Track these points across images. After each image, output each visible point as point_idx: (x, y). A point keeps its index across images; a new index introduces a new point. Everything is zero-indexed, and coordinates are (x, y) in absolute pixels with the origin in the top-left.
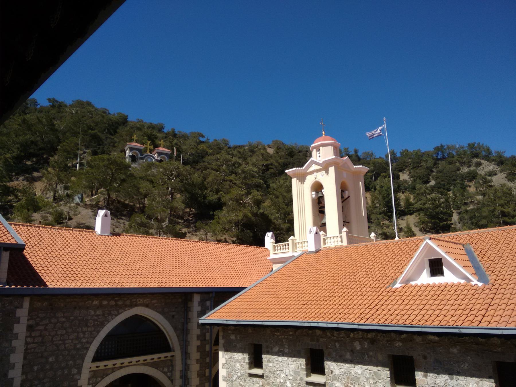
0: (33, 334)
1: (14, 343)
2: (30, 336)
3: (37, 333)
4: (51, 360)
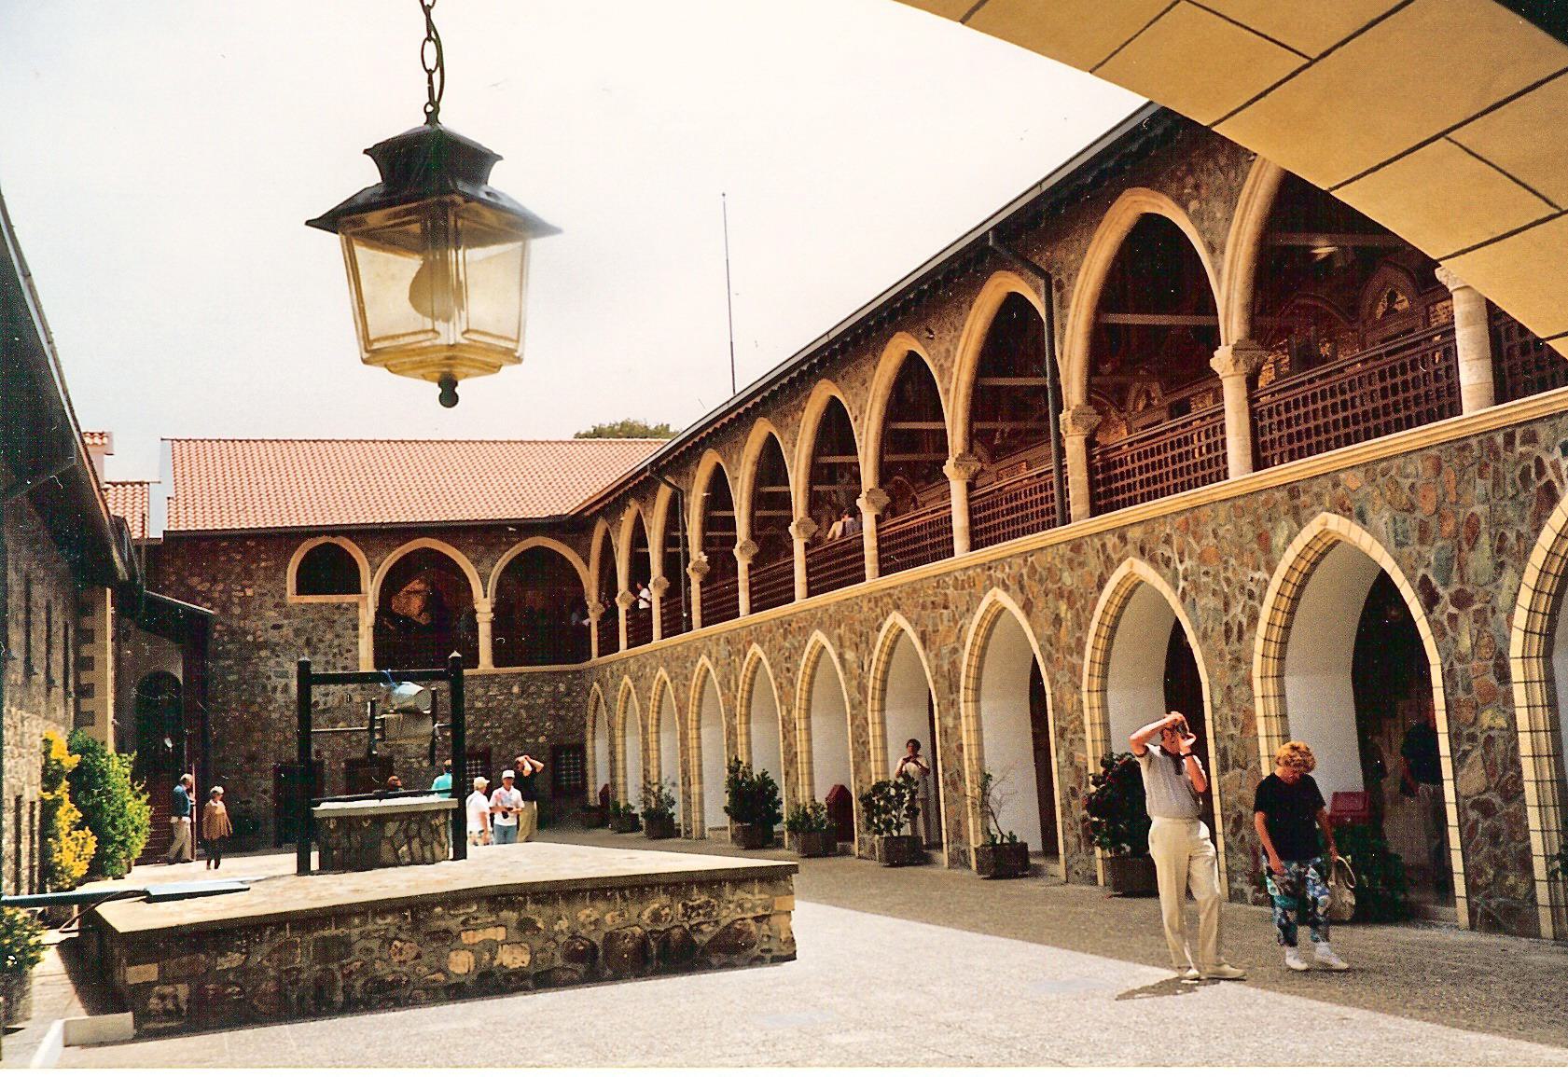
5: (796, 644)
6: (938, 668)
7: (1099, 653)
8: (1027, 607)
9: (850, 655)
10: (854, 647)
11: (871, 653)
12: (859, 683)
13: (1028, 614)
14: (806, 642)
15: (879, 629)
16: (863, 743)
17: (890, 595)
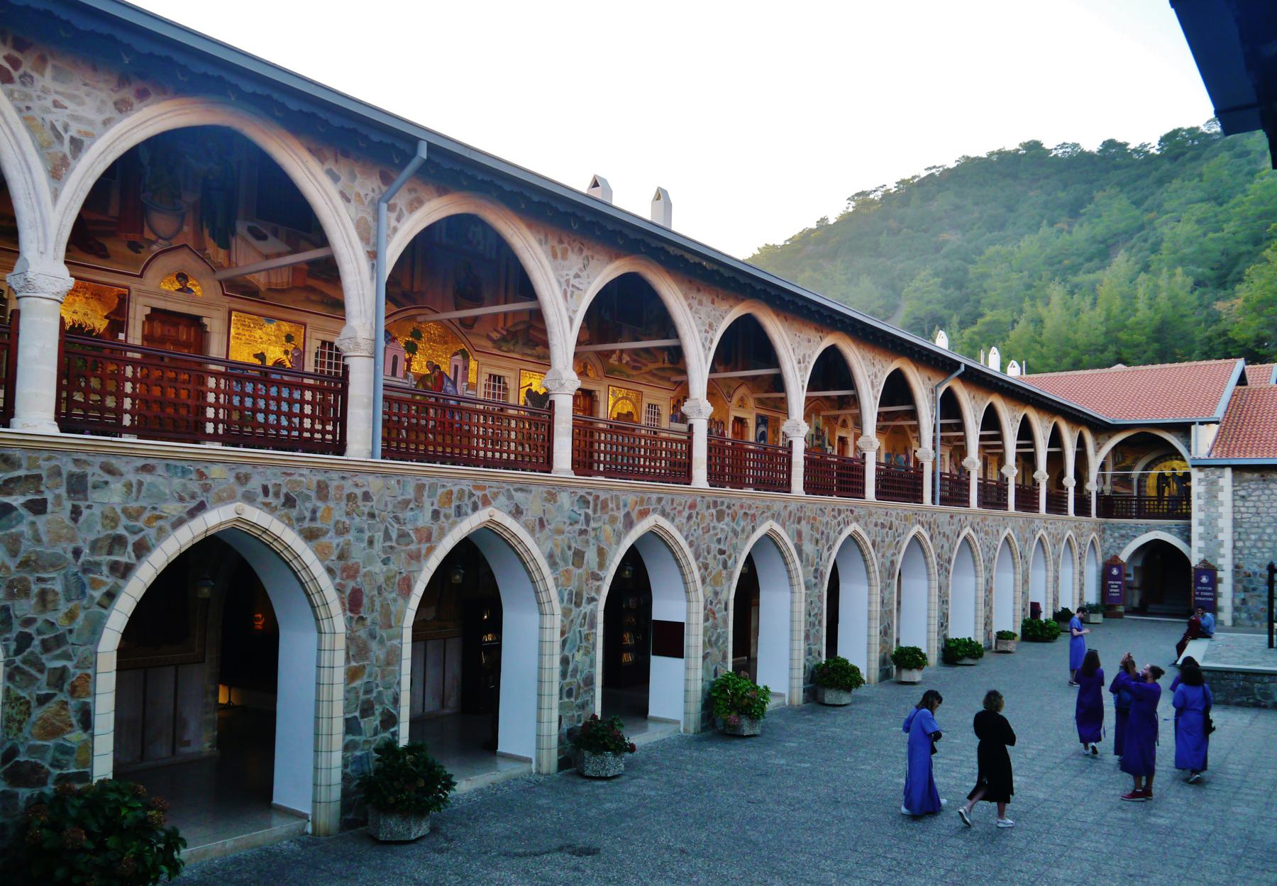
0: (1247, 504)
1: (1221, 509)
2: (1244, 506)
3: (1251, 504)
4: (1269, 531)
5: (739, 529)
8: (931, 538)
9: (808, 548)
10: (814, 542)
11: (830, 548)
12: (816, 570)
13: (931, 540)
14: (754, 529)
15: (840, 532)
16: (816, 615)
17: (852, 511)
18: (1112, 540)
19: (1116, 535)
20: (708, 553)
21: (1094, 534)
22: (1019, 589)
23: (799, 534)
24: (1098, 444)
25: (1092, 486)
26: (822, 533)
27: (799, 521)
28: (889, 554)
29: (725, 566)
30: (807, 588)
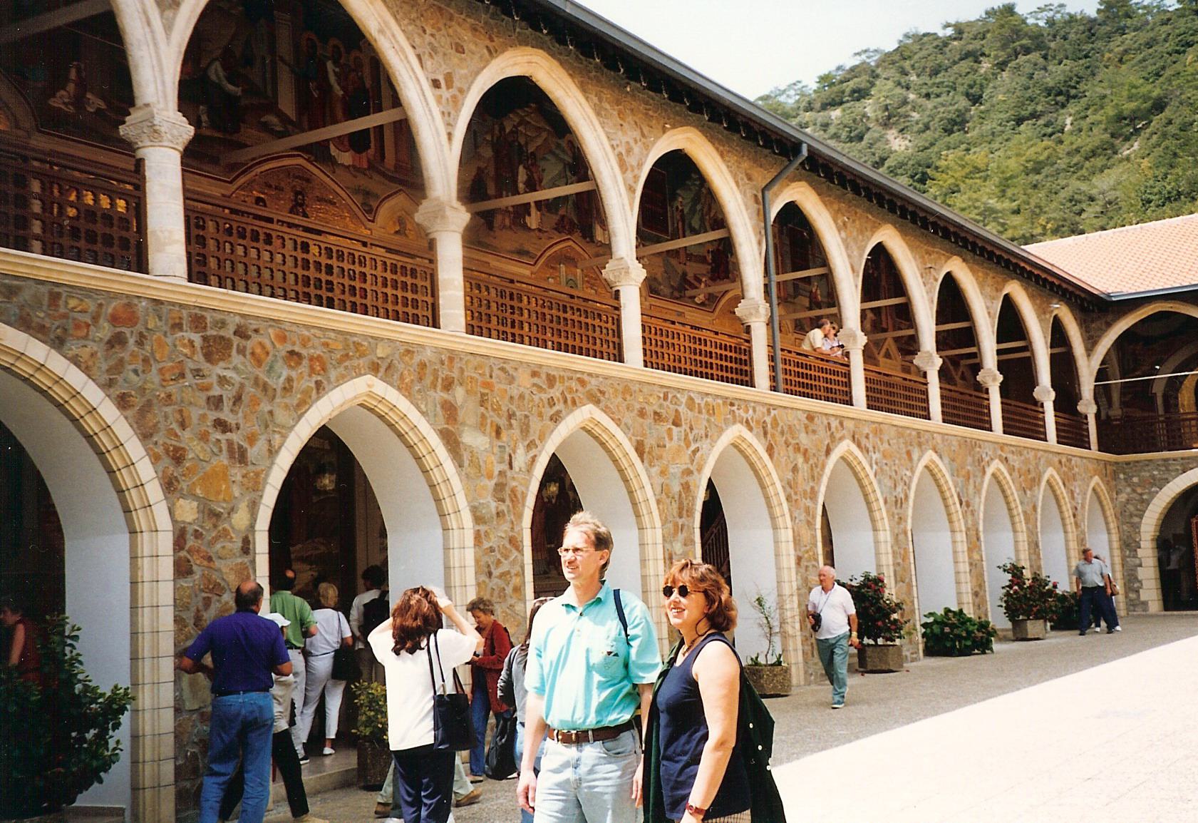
6: (664, 489)
7: (776, 503)
8: (770, 450)
9: (474, 440)
12: (500, 487)
13: (771, 456)
15: (556, 419)
18: (1129, 490)
19: (1135, 480)
20: (183, 425)
21: (1096, 478)
22: (963, 557)
23: (450, 410)
24: (1090, 338)
25: (1088, 406)
26: (511, 416)
27: (448, 385)
28: (675, 469)
29: (239, 456)
30: (478, 519)
